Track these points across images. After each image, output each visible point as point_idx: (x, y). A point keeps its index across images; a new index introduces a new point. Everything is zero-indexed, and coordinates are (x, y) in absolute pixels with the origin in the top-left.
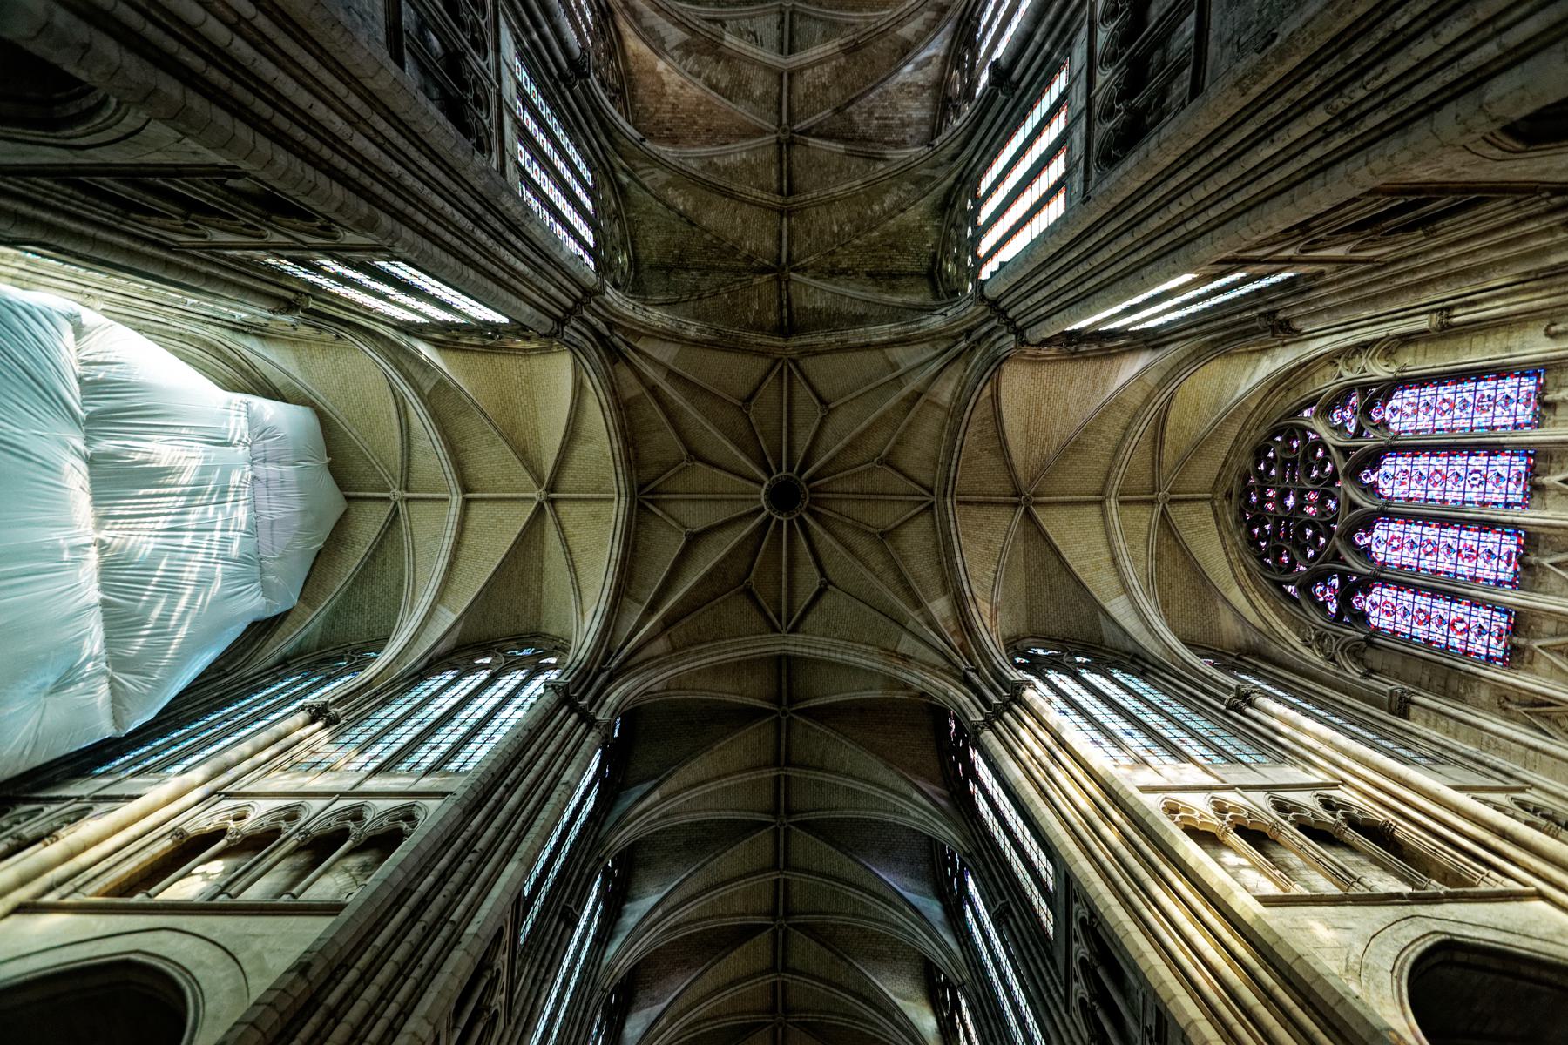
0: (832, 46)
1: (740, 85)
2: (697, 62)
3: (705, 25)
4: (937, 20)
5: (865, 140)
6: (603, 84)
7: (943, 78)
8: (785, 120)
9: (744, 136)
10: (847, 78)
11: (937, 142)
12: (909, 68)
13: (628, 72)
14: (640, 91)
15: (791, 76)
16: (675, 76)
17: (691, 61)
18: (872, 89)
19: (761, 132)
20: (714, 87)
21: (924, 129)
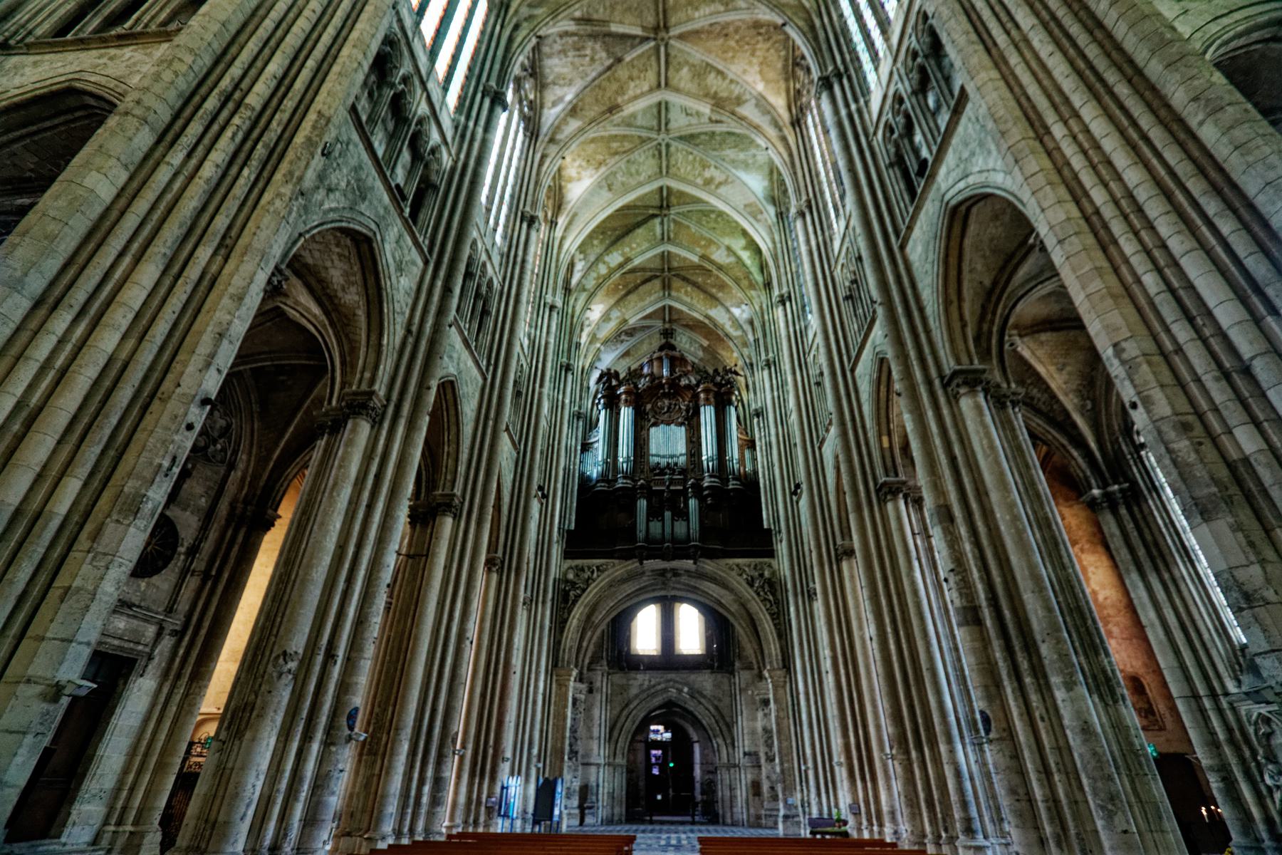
0: (629, 110)
1: (699, 75)
2: (731, 92)
3: (724, 118)
4: (554, 133)
5: (594, 36)
6: (808, 70)
7: (541, 92)
8: (662, 49)
9: (697, 32)
10: (615, 86)
11: (534, 41)
12: (569, 98)
13: (787, 80)
14: (780, 65)
15: (659, 85)
16: (749, 78)
17: (736, 92)
18: (594, 80)
19: (681, 37)
20: (719, 72)
21: (546, 49)
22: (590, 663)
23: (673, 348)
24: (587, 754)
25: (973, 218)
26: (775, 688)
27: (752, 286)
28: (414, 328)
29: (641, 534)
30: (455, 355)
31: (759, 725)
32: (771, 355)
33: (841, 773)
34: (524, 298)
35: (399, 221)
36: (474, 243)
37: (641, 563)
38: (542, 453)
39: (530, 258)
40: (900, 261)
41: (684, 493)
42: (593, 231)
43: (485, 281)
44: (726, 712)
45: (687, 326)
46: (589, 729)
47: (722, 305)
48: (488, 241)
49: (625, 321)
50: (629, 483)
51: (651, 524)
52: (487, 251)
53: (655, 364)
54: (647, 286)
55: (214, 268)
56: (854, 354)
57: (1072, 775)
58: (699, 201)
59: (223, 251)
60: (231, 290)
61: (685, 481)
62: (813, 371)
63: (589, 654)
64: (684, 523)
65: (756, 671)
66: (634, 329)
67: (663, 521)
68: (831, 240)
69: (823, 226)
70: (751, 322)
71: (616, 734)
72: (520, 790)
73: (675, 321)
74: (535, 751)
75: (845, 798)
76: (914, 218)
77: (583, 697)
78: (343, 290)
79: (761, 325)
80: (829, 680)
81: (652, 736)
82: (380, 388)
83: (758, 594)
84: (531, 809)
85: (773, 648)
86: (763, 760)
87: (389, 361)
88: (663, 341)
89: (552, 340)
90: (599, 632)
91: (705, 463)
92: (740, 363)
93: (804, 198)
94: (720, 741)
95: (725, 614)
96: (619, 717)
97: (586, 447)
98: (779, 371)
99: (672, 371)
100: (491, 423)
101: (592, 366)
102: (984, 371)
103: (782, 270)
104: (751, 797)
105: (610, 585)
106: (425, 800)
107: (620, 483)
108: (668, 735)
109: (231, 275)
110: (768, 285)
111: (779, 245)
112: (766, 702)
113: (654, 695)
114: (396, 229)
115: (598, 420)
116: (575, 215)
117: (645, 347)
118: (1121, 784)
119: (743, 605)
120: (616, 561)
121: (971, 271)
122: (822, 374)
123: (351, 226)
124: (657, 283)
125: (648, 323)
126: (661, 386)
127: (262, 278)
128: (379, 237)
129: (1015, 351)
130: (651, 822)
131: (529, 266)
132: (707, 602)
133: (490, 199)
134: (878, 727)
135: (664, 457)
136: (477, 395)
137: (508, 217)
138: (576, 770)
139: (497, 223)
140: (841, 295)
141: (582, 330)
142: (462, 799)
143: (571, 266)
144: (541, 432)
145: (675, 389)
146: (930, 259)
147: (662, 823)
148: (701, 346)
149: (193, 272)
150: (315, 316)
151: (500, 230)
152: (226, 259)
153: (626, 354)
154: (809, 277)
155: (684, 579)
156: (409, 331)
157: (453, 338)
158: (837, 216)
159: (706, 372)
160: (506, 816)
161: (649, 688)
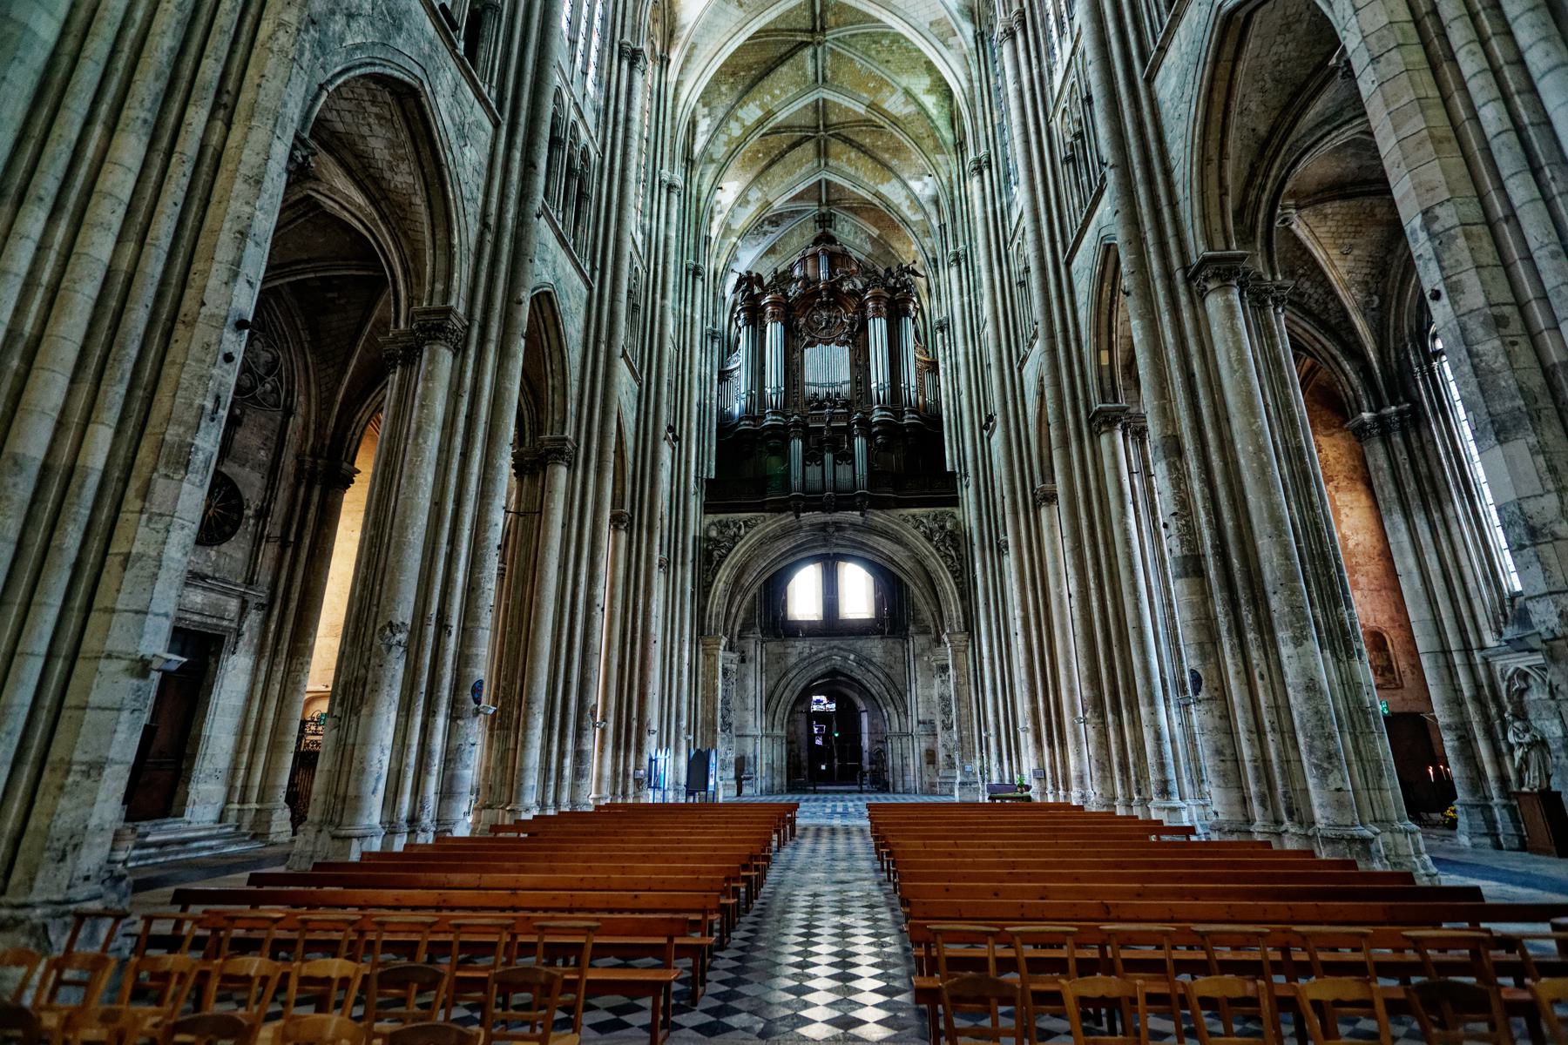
23: (831, 240)
24: (742, 726)
25: (1254, 29)
26: (955, 652)
27: (938, 148)
28: (492, 221)
29: (796, 481)
30: (549, 257)
31: (935, 693)
32: (961, 246)
33: (1027, 740)
34: (632, 174)
35: (451, 63)
36: (558, 93)
37: (797, 517)
38: (669, 384)
39: (636, 115)
40: (1144, 103)
41: (848, 430)
42: (719, 71)
43: (578, 150)
44: (897, 679)
45: (850, 209)
46: (743, 700)
47: (898, 177)
48: (577, 90)
49: (768, 204)
50: (779, 420)
51: (808, 469)
52: (576, 104)
53: (809, 263)
54: (797, 152)
55: (215, 139)
56: (1071, 241)
57: (1287, 734)
58: (868, 18)
59: (221, 113)
60: (243, 170)
61: (849, 415)
62: (1016, 267)
63: (739, 621)
64: (849, 468)
66: (781, 214)
67: (823, 464)
68: (1051, 73)
69: (1039, 52)
70: (936, 201)
71: (773, 704)
72: (670, 762)
73: (834, 202)
74: (684, 723)
75: (1029, 762)
76: (1170, 33)
77: (734, 667)
78: (391, 169)
79: (950, 204)
80: (1018, 644)
81: (815, 708)
82: (458, 304)
83: (938, 550)
84: (683, 780)
85: (954, 609)
86: (939, 729)
87: (465, 266)
88: (820, 231)
89: (673, 234)
91: (874, 392)
92: (920, 259)
93: (1016, 7)
94: (891, 709)
95: (899, 573)
96: (776, 686)
97: (724, 376)
98: (972, 268)
99: (832, 272)
100: (603, 347)
101: (727, 269)
102: (1243, 257)
103: (980, 122)
104: (924, 765)
105: (761, 543)
106: (568, 772)
107: (769, 420)
108: (833, 706)
109: (240, 149)
110: (960, 146)
111: (976, 84)
112: (944, 669)
113: (814, 664)
114: (449, 76)
115: (738, 340)
116: (694, 46)
117: (795, 241)
118: (1342, 743)
119: (920, 563)
120: (767, 515)
121: (1241, 113)
122: (1027, 270)
123: (388, 71)
124: (809, 147)
125: (798, 205)
126: (818, 293)
127: (281, 151)
128: (428, 88)
129: (1288, 229)
130: (815, 792)
131: (635, 127)
132: (877, 560)
133: (574, 25)
134: (1071, 691)
135: (823, 386)
136: (582, 311)
137: (600, 52)
138: (730, 742)
139: (586, 63)
140: (1060, 153)
141: (711, 219)
142: (608, 771)
143: (693, 125)
144: (666, 358)
145: (835, 296)
146: (1186, 98)
147: (827, 792)
148: (870, 236)
149: (189, 145)
150: (359, 207)
151: (592, 71)
152: (228, 125)
153: (771, 251)
154: (1016, 131)
155: (849, 534)
156: (485, 225)
157: (544, 234)
158: (1060, 36)
159: (876, 272)
160: (656, 787)
161: (810, 656)
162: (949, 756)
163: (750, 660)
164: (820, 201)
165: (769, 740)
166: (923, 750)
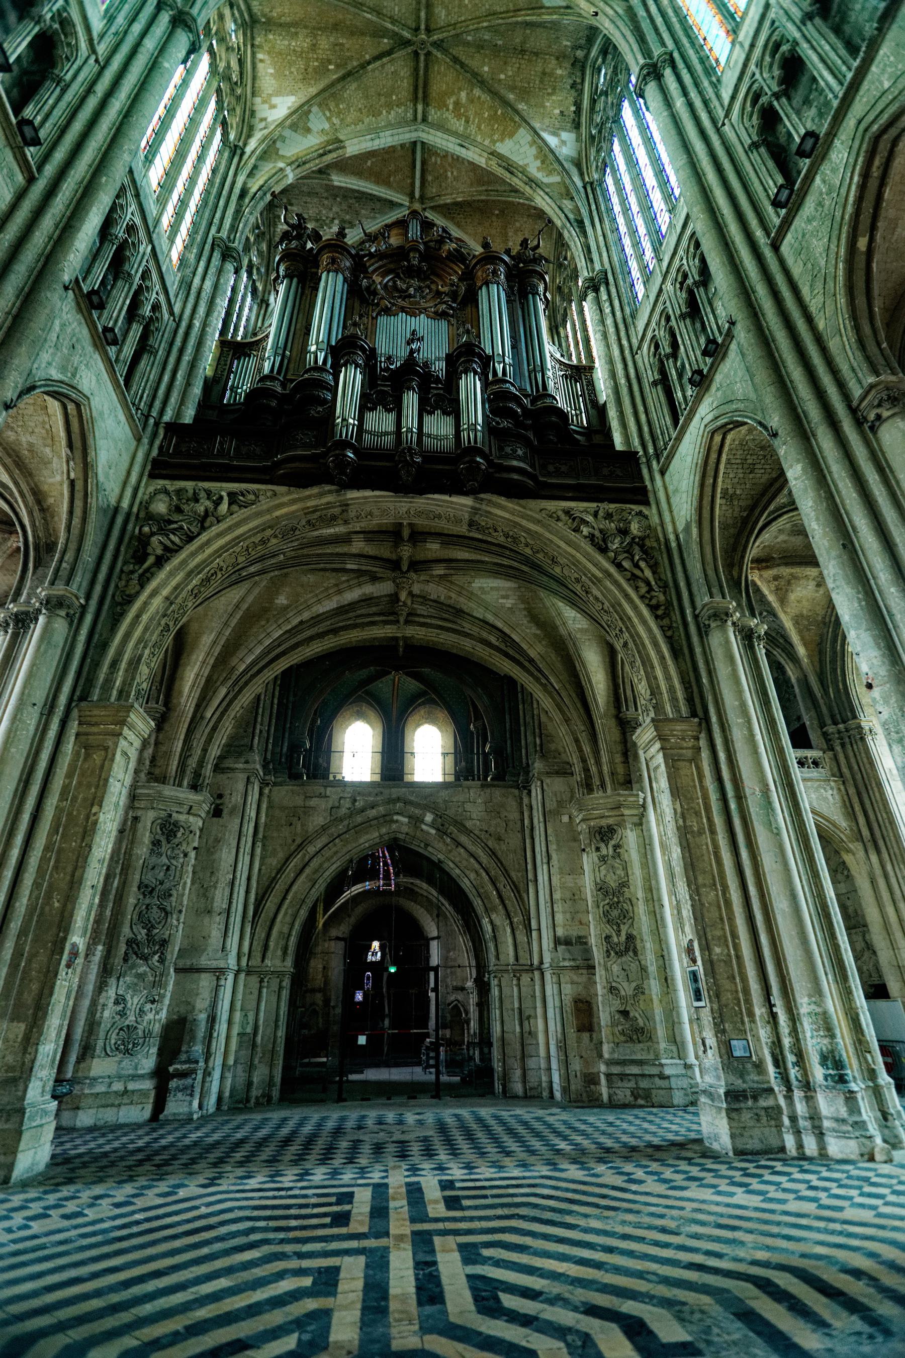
22: (221, 758)
44: (510, 860)
46: (204, 891)
65: (579, 776)
71: (270, 905)
77: (197, 823)
86: (598, 955)
90: (246, 698)
94: (499, 919)
96: (280, 871)
104: (571, 1032)
113: (359, 829)
138: (158, 983)
161: (351, 814)
162: (625, 1013)
163: (232, 812)
164: (411, 196)
165: (254, 980)
166: (568, 1000)
